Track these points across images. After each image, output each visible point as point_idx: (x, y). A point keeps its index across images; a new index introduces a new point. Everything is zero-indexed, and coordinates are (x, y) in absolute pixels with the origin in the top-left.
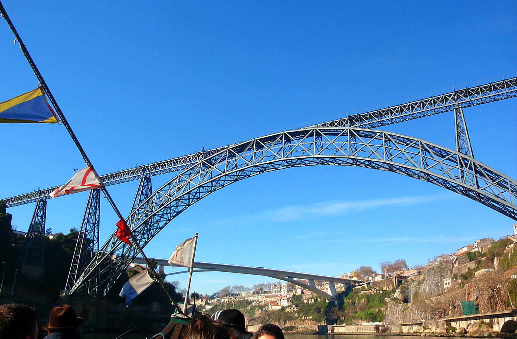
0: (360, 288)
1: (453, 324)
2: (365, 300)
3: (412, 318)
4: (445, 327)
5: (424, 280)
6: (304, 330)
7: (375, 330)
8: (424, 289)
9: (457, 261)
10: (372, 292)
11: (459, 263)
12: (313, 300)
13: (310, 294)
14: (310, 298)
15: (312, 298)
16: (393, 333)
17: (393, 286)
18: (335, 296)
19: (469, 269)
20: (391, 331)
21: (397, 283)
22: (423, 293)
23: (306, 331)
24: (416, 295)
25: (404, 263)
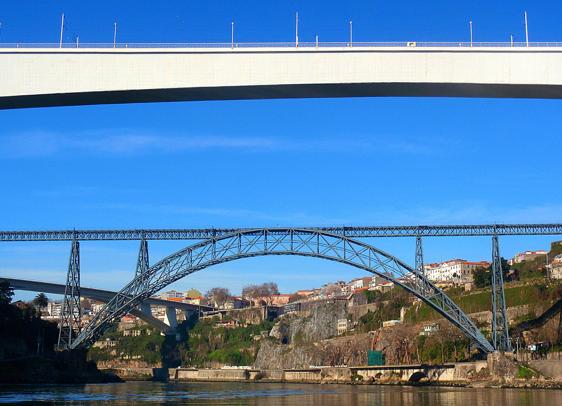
0: (212, 318)
1: (359, 373)
2: (222, 336)
3: (295, 363)
4: (350, 375)
5: (311, 317)
6: (132, 375)
7: (244, 376)
8: (310, 328)
9: (353, 299)
10: (232, 325)
11: (355, 301)
12: (139, 332)
13: (130, 322)
14: (132, 329)
15: (136, 328)
16: (272, 380)
17: (261, 319)
18: (176, 327)
19: (369, 311)
20: (269, 378)
21: (266, 315)
22: (309, 333)
23: (134, 376)
24: (299, 334)
25: (274, 287)
